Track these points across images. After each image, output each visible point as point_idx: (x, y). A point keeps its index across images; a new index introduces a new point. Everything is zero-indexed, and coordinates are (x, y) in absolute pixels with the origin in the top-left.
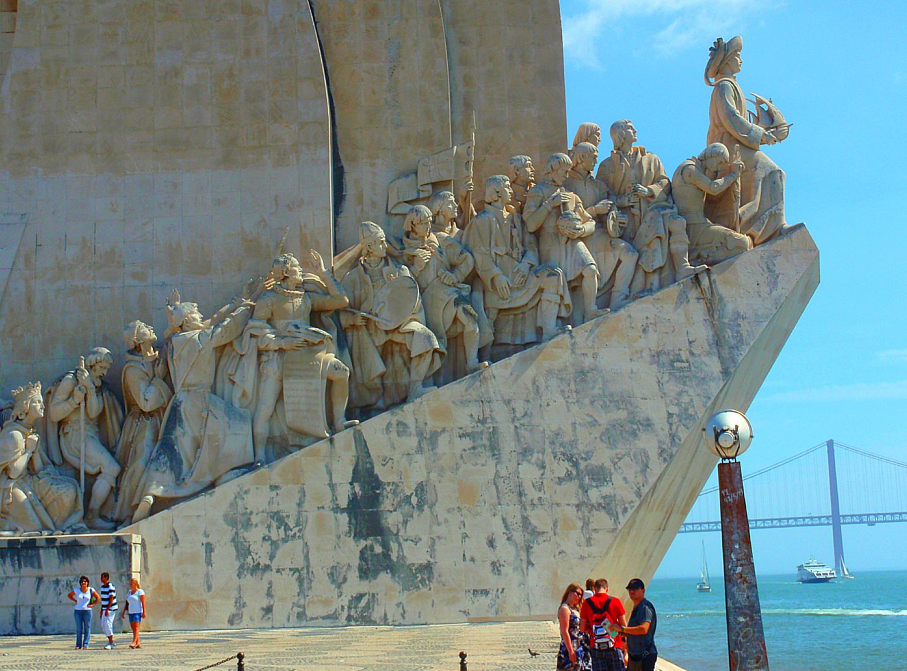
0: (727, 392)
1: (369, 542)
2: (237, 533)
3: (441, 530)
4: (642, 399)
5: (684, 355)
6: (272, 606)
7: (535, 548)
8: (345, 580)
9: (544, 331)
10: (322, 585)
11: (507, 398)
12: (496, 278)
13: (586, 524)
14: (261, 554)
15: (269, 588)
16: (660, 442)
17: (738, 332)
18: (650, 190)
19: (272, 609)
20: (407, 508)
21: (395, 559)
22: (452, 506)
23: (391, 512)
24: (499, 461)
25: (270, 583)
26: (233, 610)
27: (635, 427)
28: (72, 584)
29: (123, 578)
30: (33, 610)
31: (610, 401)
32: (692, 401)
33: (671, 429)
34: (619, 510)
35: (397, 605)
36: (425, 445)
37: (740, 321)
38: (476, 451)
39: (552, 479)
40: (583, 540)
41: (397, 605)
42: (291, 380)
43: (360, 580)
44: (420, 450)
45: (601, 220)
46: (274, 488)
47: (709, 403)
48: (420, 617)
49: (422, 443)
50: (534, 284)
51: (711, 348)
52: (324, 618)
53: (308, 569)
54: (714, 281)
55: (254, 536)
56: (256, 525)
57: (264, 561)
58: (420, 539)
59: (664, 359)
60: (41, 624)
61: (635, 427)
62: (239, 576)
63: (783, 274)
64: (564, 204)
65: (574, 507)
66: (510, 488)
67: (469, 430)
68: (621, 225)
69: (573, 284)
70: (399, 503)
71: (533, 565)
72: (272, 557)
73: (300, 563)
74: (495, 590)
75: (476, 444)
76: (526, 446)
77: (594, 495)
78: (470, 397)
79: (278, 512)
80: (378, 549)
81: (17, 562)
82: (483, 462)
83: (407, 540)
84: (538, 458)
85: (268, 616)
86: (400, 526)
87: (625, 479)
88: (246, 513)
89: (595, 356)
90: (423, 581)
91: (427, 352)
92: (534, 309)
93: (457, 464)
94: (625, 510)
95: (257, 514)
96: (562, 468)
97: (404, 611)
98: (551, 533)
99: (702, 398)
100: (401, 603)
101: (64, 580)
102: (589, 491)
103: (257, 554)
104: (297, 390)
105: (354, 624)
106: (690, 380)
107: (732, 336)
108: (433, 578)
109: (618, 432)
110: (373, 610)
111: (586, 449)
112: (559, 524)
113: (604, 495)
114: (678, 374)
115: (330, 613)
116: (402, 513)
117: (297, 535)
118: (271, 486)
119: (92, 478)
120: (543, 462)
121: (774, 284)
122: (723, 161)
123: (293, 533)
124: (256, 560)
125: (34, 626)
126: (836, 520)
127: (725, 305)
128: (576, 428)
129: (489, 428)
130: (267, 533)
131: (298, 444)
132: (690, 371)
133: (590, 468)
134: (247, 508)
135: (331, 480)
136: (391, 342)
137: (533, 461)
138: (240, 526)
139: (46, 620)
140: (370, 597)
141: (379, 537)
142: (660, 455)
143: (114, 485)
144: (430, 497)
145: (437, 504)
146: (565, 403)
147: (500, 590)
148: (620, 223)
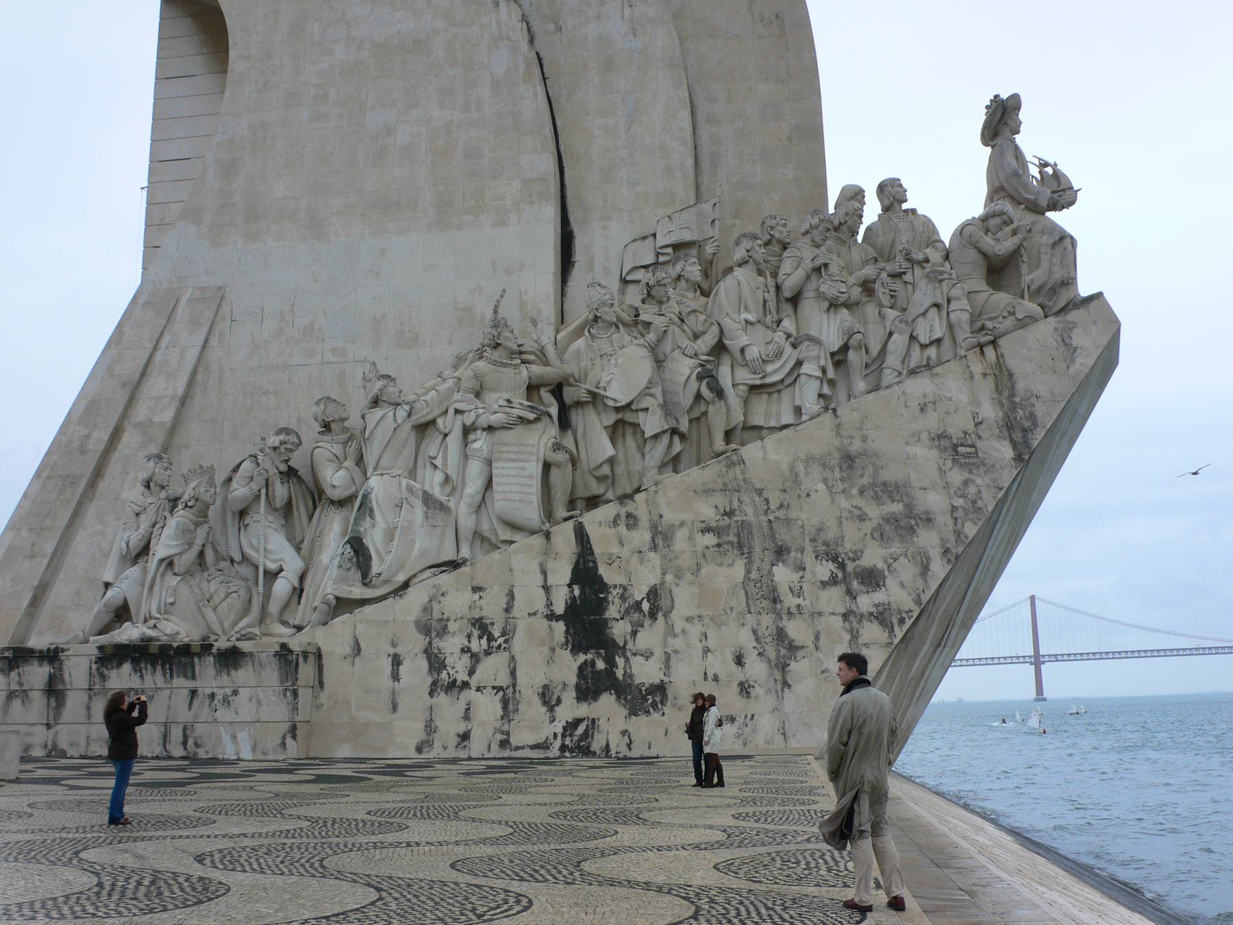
0: (1019, 483)
1: (589, 656)
2: (430, 643)
3: (678, 643)
4: (920, 489)
6: (469, 731)
7: (794, 666)
8: (559, 701)
9: (803, 411)
10: (532, 709)
11: (758, 486)
14: (458, 667)
16: (942, 539)
17: (1031, 414)
18: (925, 254)
19: (469, 735)
21: (621, 678)
22: (690, 614)
23: (617, 620)
25: (469, 704)
26: (423, 736)
27: (913, 522)
28: (230, 698)
29: (288, 693)
30: (185, 729)
31: (883, 492)
32: (980, 492)
33: (956, 525)
34: (895, 621)
35: (622, 733)
37: (1034, 400)
38: (722, 549)
39: (813, 584)
41: (622, 733)
42: (502, 465)
43: (578, 702)
44: (654, 547)
45: (867, 287)
47: (1001, 494)
48: (650, 748)
49: (656, 538)
51: (1001, 432)
52: (533, 747)
53: (514, 688)
54: (1002, 356)
55: (451, 645)
56: (454, 633)
57: (462, 676)
58: (652, 654)
59: (944, 443)
60: (193, 746)
61: (913, 522)
62: (431, 694)
63: (1081, 348)
64: (826, 265)
65: (840, 616)
66: (762, 593)
67: (713, 524)
68: (892, 293)
69: (837, 358)
70: (627, 612)
71: (789, 686)
72: (471, 672)
73: (503, 680)
74: (743, 717)
75: (721, 541)
76: (781, 543)
77: (865, 602)
78: (715, 485)
79: (481, 619)
80: (601, 665)
81: (168, 671)
82: (730, 562)
83: (635, 655)
84: (796, 559)
85: (466, 743)
86: (628, 637)
87: (902, 584)
88: (441, 620)
89: (864, 439)
90: (654, 705)
91: (664, 432)
92: (792, 387)
93: (698, 564)
94: (902, 621)
95: (455, 621)
96: (825, 570)
97: (630, 740)
98: (812, 647)
99: (992, 489)
100: (627, 731)
101: (220, 694)
102: (858, 598)
103: (453, 668)
105: (569, 756)
106: (978, 467)
107: (1025, 417)
108: (667, 701)
109: (893, 528)
110: (592, 737)
111: (854, 548)
112: (822, 637)
113: (877, 602)
114: (962, 460)
115: (540, 741)
116: (631, 622)
117: (503, 647)
119: (272, 576)
121: (1071, 361)
123: (498, 643)
125: (185, 748)
127: (1015, 383)
128: (842, 522)
129: (737, 521)
130: (467, 643)
131: (509, 539)
133: (858, 570)
135: (546, 581)
139: (199, 742)
140: (589, 723)
141: (601, 651)
143: (296, 585)
144: (664, 603)
145: (673, 612)
146: (828, 493)
147: (749, 716)
148: (891, 290)
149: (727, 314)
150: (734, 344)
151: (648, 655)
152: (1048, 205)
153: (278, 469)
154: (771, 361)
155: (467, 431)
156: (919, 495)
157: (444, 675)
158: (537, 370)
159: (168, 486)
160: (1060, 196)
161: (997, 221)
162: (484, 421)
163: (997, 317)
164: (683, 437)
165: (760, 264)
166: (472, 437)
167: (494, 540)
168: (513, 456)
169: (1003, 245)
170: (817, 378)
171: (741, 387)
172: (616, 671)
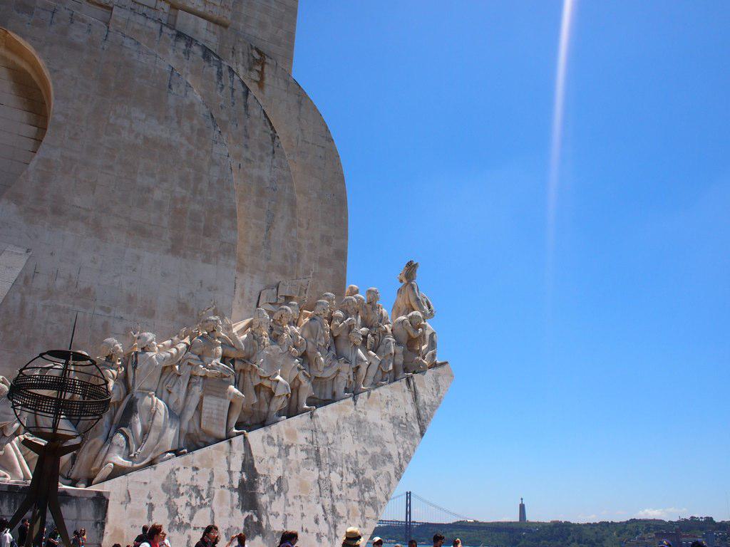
1: (250, 514)
3: (290, 510)
5: (404, 421)
7: (339, 526)
13: (363, 513)
14: (184, 513)
15: (188, 541)
16: (396, 468)
20: (272, 493)
22: (296, 494)
24: (320, 470)
25: (189, 537)
29: (98, 525)
36: (283, 453)
40: (362, 525)
42: (209, 397)
44: (279, 456)
46: (196, 469)
50: (336, 365)
55: (181, 502)
56: (183, 494)
57: (186, 520)
72: (191, 518)
80: (255, 519)
89: (365, 414)
96: (351, 478)
98: (346, 518)
112: (350, 513)
118: (193, 468)
120: (342, 472)
132: (407, 430)
134: (177, 481)
135: (229, 468)
136: (261, 385)
137: (337, 470)
138: (172, 493)
142: (396, 476)
144: (284, 487)
151: (277, 515)
156: (387, 444)
157: (177, 518)
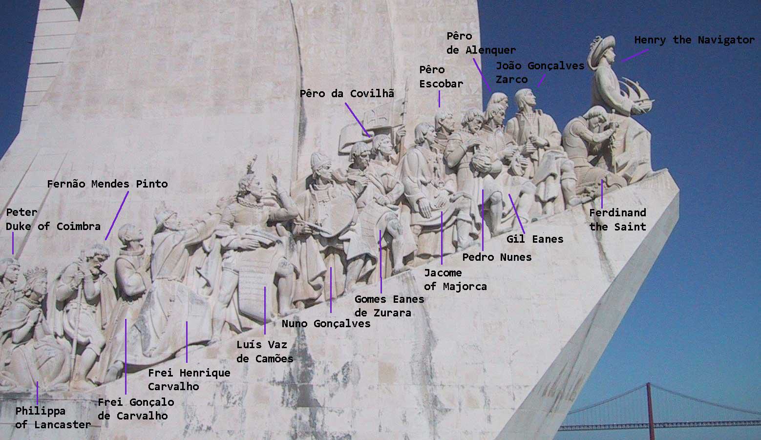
12: (420, 200)
20: (333, 383)
58: (343, 411)
64: (477, 146)
80: (306, 419)
83: (331, 411)
91: (360, 256)
104: (250, 283)
117: (237, 403)
119: (81, 348)
122: (603, 118)
124: (201, 422)
126: (651, 426)
144: (352, 375)
148: (522, 164)
149: (409, 177)
150: (413, 197)
152: (631, 110)
153: (91, 272)
154: (437, 210)
155: (223, 250)
158: (276, 209)
159: (16, 281)
160: (640, 105)
161: (597, 119)
162: (235, 244)
163: (594, 184)
164: (374, 261)
165: (432, 143)
166: (226, 254)
167: (238, 328)
168: (255, 270)
169: (600, 137)
170: (468, 222)
171: (416, 227)
172: (317, 423)
